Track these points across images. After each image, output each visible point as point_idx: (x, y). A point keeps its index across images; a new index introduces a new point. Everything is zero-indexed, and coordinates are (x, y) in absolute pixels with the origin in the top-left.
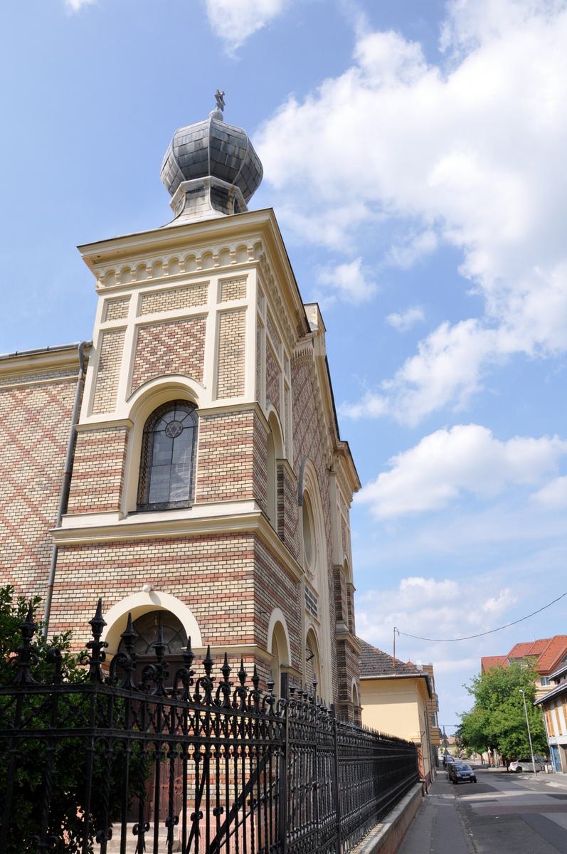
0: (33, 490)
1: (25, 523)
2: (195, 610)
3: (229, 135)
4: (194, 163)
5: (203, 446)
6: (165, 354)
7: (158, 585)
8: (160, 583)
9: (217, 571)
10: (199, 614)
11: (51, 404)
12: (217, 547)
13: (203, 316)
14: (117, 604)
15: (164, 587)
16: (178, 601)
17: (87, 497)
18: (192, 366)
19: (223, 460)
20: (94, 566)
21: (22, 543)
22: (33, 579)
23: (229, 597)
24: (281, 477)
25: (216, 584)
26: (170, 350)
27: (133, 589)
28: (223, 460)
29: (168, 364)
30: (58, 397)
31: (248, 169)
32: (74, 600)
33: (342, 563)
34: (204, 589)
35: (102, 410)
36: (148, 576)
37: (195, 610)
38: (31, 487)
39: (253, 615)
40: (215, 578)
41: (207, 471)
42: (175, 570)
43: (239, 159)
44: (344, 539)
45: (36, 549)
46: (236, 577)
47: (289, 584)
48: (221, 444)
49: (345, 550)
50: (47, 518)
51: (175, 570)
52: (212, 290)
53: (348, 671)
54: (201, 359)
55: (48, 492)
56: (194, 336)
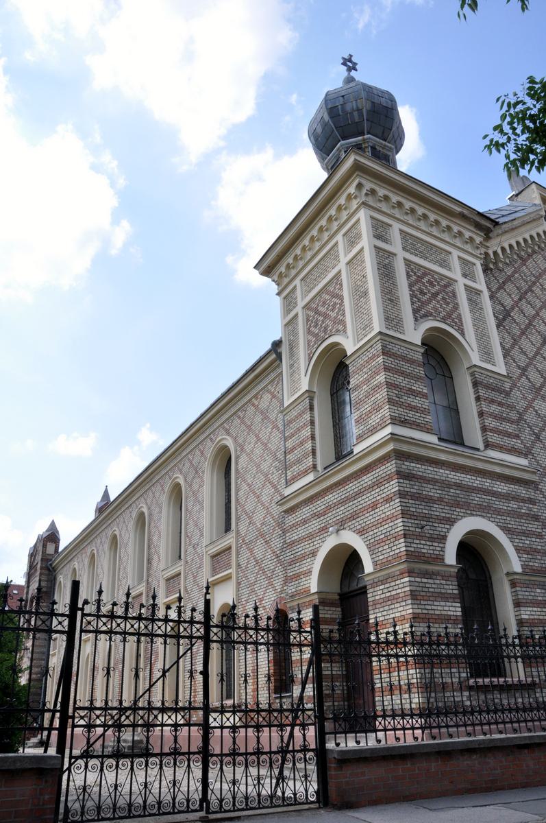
0: (273, 473)
2: (366, 540)
3: (343, 96)
4: (327, 140)
8: (343, 523)
10: (368, 542)
14: (321, 549)
15: (346, 526)
20: (305, 522)
22: (281, 544)
25: (376, 511)
29: (325, 331)
31: (374, 112)
32: (298, 554)
36: (334, 519)
37: (366, 540)
39: (402, 532)
40: (374, 506)
41: (359, 412)
43: (359, 110)
46: (388, 500)
48: (363, 383)
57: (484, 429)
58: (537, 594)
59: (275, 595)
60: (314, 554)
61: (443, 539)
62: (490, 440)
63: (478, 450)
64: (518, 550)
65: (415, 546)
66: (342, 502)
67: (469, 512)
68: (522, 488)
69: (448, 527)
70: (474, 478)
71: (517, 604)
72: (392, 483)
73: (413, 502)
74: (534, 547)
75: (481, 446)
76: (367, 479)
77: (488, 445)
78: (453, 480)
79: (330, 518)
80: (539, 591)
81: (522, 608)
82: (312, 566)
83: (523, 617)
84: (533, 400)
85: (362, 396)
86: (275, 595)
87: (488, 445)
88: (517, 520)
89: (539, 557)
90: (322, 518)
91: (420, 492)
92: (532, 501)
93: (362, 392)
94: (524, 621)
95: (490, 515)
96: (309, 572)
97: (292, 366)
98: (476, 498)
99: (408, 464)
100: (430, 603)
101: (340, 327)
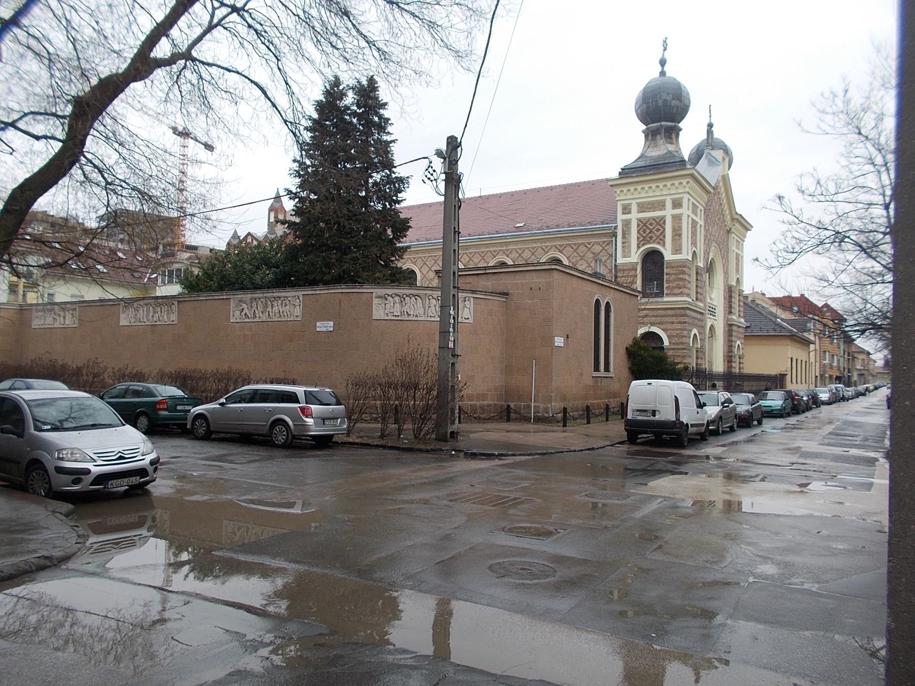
5: (667, 274)
6: (649, 233)
7: (653, 324)
13: (663, 219)
18: (661, 239)
19: (675, 280)
23: (677, 329)
24: (697, 273)
28: (675, 280)
29: (651, 238)
33: (734, 283)
34: (669, 326)
40: (673, 323)
42: (659, 319)
44: (737, 264)
47: (699, 316)
48: (674, 274)
49: (737, 270)
51: (659, 319)
52: (669, 204)
53: (733, 338)
54: (664, 237)
56: (660, 225)
76: (670, 312)
79: (646, 320)
97: (623, 243)
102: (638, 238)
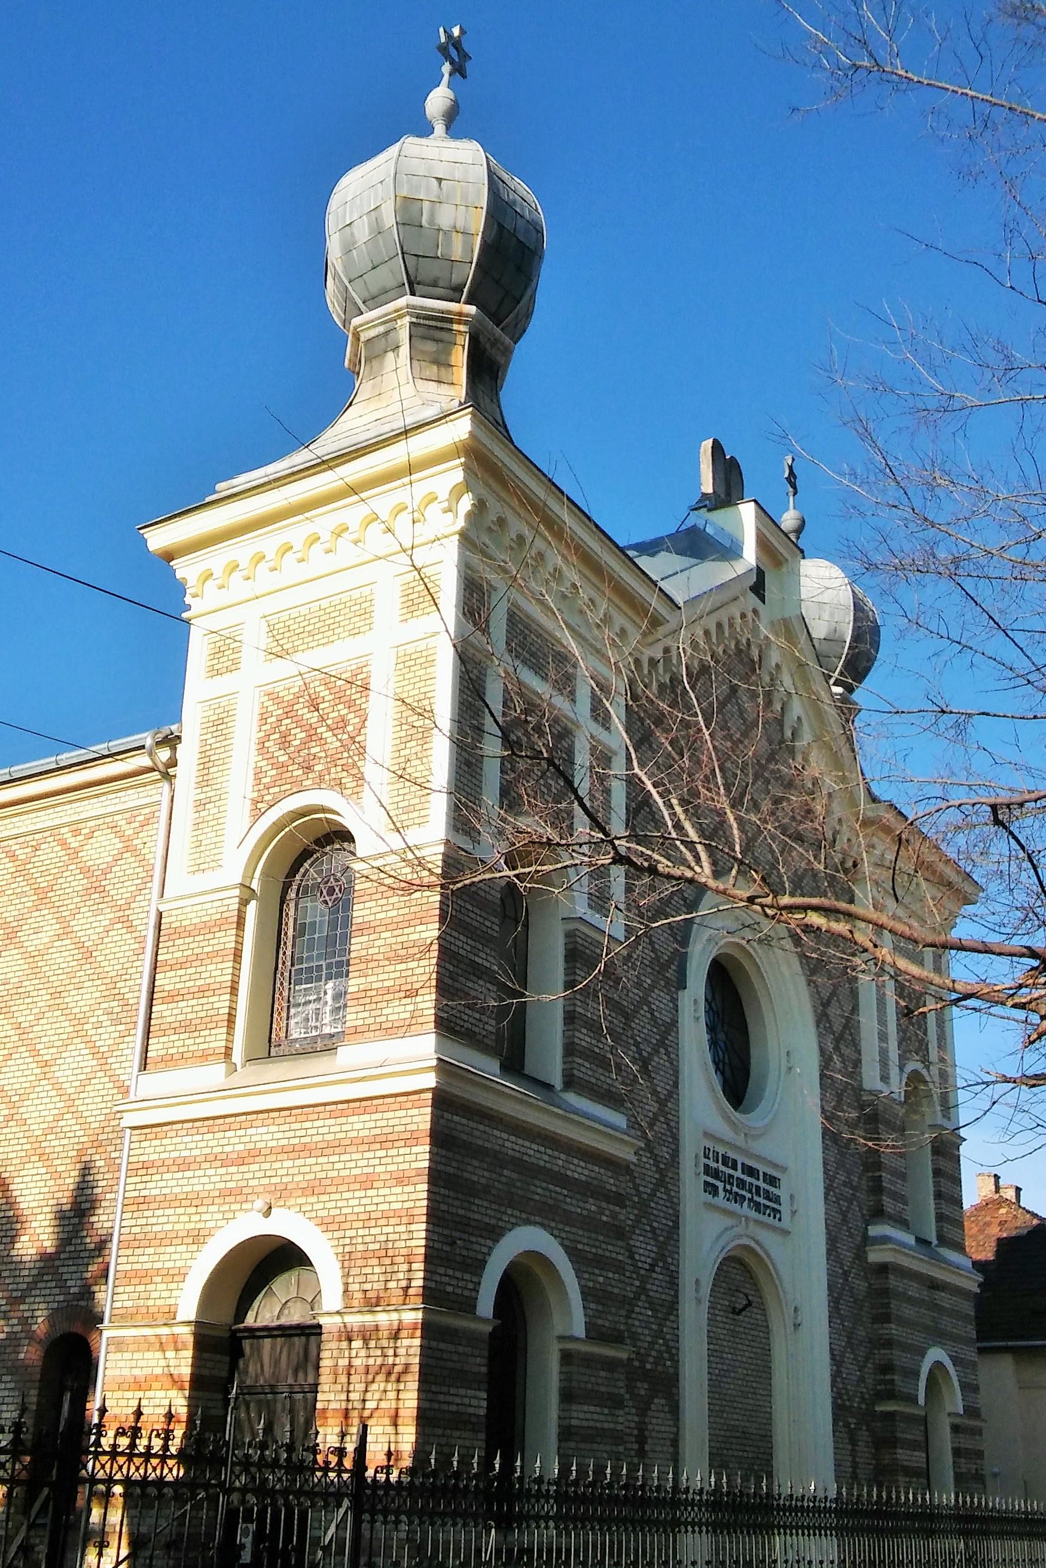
0: (99, 1025)
1: (88, 1088)
9: (371, 1170)
11: (125, 856)
12: (372, 1124)
14: (218, 1233)
15: (292, 1202)
16: (311, 1224)
17: (176, 1037)
20: (184, 1165)
21: (84, 1124)
25: (370, 1193)
26: (312, 735)
27: (244, 1206)
30: (135, 842)
34: (354, 1202)
35: (202, 867)
38: (95, 1019)
40: (367, 1182)
41: (363, 980)
45: (105, 1136)
46: (401, 1180)
50: (122, 1078)
55: (122, 1027)
57: (570, 1049)
58: (600, 1381)
59: (61, 1298)
60: (198, 1238)
61: (478, 1266)
62: (576, 1072)
63: (549, 1087)
64: (587, 1294)
65: (438, 1278)
66: (293, 1151)
67: (524, 1216)
68: (610, 1174)
69: (489, 1243)
70: (542, 1149)
71: (567, 1397)
72: (415, 1149)
73: (447, 1192)
74: (609, 1289)
75: (557, 1082)
76: (360, 1124)
77: (570, 1082)
78: (510, 1152)
79: (253, 1174)
80: (603, 1374)
81: (574, 1407)
82: (189, 1263)
83: (574, 1422)
84: (652, 987)
85: (376, 950)
86: (61, 1298)
87: (570, 1082)
88: (593, 1235)
89: (613, 1310)
90: (233, 1169)
91: (460, 1173)
92: (619, 1199)
93: (377, 943)
94: (573, 1430)
95: (553, 1224)
96: (179, 1275)
97: (200, 805)
98: (539, 1190)
99: (449, 1116)
100: (445, 1389)
101: (348, 781)
102: (258, 775)
